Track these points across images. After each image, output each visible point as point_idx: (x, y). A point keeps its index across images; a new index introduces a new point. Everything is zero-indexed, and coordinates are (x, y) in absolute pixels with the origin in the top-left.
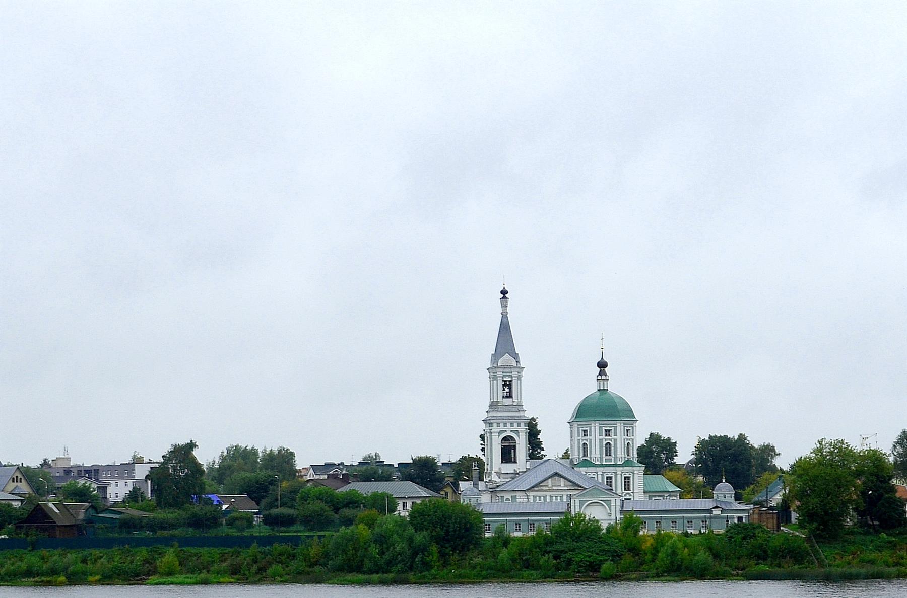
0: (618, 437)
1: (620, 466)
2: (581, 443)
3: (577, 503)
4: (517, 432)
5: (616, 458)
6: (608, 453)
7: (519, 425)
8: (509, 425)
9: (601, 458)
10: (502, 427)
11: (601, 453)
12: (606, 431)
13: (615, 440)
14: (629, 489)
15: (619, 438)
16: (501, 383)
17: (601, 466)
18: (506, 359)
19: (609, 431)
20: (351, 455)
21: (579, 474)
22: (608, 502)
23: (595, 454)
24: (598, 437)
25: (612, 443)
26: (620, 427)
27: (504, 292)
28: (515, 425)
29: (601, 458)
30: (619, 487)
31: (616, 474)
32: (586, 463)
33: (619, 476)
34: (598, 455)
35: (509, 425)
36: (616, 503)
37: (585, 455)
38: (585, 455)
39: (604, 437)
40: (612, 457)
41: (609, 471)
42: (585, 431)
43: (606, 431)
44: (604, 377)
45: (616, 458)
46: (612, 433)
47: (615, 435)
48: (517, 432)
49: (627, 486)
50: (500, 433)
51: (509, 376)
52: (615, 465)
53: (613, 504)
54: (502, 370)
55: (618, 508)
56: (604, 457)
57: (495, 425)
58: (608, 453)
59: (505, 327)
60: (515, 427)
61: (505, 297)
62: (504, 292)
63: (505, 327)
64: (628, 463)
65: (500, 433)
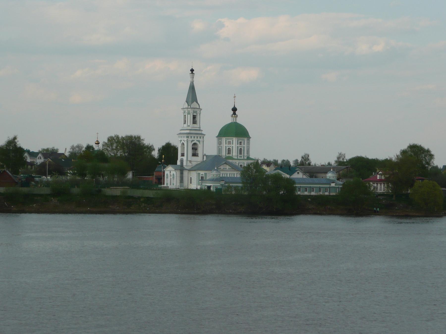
2: (227, 148)
4: (199, 141)
5: (244, 156)
6: (241, 153)
7: (200, 138)
9: (238, 155)
10: (193, 139)
11: (238, 153)
13: (244, 147)
17: (238, 159)
18: (194, 105)
20: (293, 156)
25: (243, 148)
27: (192, 70)
28: (199, 137)
29: (238, 155)
31: (244, 163)
35: (196, 137)
37: (229, 153)
38: (229, 153)
45: (244, 156)
46: (242, 143)
47: (244, 144)
48: (199, 141)
50: (192, 141)
52: (244, 159)
54: (193, 110)
56: (239, 155)
57: (190, 137)
58: (241, 153)
59: (192, 88)
61: (192, 73)
62: (192, 70)
63: (192, 88)
65: (192, 141)
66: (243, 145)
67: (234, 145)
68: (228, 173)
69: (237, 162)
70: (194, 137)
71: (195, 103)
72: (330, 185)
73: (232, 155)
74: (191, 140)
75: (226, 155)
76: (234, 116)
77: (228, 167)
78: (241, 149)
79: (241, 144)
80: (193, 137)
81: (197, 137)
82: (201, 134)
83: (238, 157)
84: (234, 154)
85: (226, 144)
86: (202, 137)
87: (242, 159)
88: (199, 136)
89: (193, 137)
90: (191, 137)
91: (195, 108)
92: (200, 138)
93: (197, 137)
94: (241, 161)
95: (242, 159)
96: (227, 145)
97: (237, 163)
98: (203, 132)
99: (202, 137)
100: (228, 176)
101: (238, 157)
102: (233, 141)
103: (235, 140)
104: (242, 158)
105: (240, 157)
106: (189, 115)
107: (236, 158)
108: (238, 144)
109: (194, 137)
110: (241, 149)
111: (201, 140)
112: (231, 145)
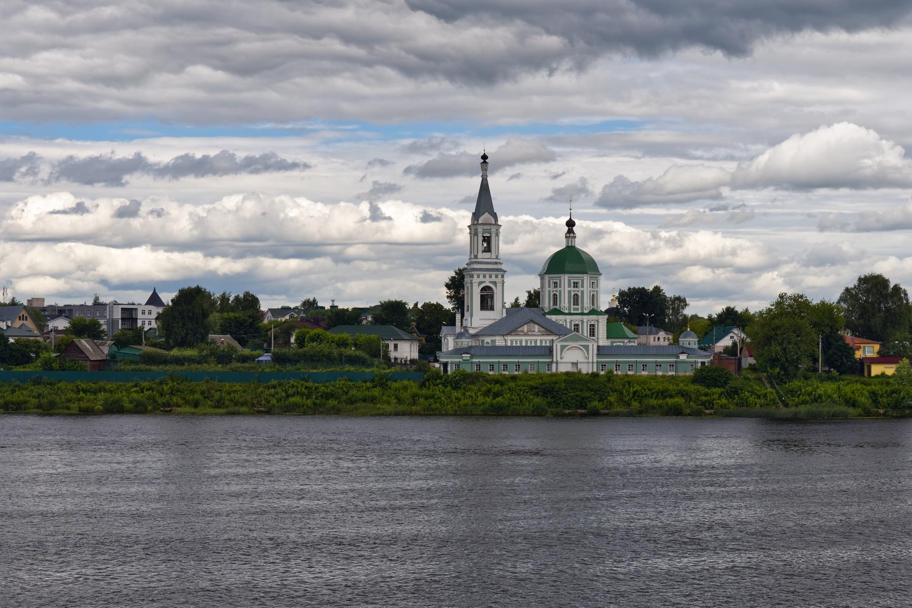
0: (585, 289)
1: (586, 314)
3: (559, 348)
4: (495, 283)
5: (582, 307)
6: (576, 302)
7: (497, 276)
10: (481, 279)
13: (582, 292)
14: (594, 335)
15: (586, 290)
16: (481, 239)
17: (570, 314)
18: (485, 217)
21: (550, 320)
22: (587, 347)
23: (565, 303)
24: (567, 289)
25: (580, 294)
26: (586, 278)
28: (493, 276)
30: (586, 332)
31: (582, 322)
33: (585, 324)
34: (567, 305)
36: (593, 347)
37: (555, 303)
38: (555, 303)
39: (572, 289)
40: (579, 307)
41: (577, 319)
42: (555, 283)
47: (583, 286)
48: (495, 283)
49: (592, 333)
50: (480, 283)
52: (582, 314)
53: (590, 348)
55: (595, 352)
56: (572, 307)
57: (475, 276)
58: (576, 302)
60: (494, 279)
61: (485, 162)
64: (593, 312)
65: (480, 283)
67: (562, 289)
68: (539, 338)
69: (569, 318)
70: (484, 276)
71: (486, 215)
72: (678, 357)
74: (479, 280)
79: (556, 287)
80: (481, 276)
81: (490, 276)
82: (498, 270)
86: (500, 276)
88: (494, 274)
89: (481, 276)
90: (478, 276)
92: (497, 276)
93: (490, 276)
97: (568, 320)
98: (503, 267)
99: (500, 276)
100: (538, 344)
103: (565, 278)
107: (567, 311)
108: (569, 286)
109: (484, 276)
111: (500, 279)
112: (558, 289)
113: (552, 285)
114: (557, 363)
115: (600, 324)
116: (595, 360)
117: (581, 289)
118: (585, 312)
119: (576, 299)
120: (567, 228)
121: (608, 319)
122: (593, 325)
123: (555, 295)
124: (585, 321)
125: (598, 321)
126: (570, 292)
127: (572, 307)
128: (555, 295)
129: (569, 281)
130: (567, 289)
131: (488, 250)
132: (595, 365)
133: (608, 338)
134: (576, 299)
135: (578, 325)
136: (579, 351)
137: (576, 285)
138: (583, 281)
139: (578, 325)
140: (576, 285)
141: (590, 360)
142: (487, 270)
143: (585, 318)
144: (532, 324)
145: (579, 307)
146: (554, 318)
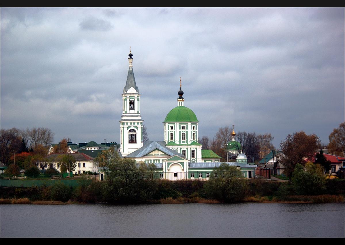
0: (189, 130)
2: (170, 133)
4: (137, 127)
5: (187, 141)
6: (184, 138)
7: (138, 123)
8: (132, 123)
9: (180, 141)
10: (129, 125)
12: (182, 127)
13: (187, 132)
14: (194, 157)
16: (128, 102)
17: (180, 145)
19: (184, 127)
21: (169, 149)
22: (182, 164)
23: (177, 138)
24: (178, 130)
25: (186, 133)
27: (131, 55)
28: (136, 123)
29: (180, 141)
30: (189, 155)
31: (187, 149)
32: (173, 144)
33: (189, 150)
34: (178, 140)
35: (132, 123)
36: (186, 163)
37: (172, 138)
38: (172, 138)
39: (181, 130)
40: (186, 140)
42: (172, 127)
43: (182, 127)
44: (181, 99)
45: (187, 141)
46: (185, 128)
47: (187, 129)
50: (128, 128)
51: (133, 98)
53: (185, 164)
54: (129, 95)
55: (188, 167)
56: (182, 140)
57: (125, 123)
58: (184, 138)
60: (136, 125)
62: (131, 55)
64: (193, 143)
65: (128, 128)
66: (186, 130)
67: (175, 130)
69: (179, 147)
70: (131, 123)
73: (174, 141)
74: (127, 126)
75: (169, 141)
76: (179, 100)
77: (160, 153)
78: (183, 134)
80: (129, 123)
81: (134, 123)
83: (180, 142)
84: (176, 140)
85: (168, 129)
87: (185, 145)
89: (129, 123)
90: (127, 124)
91: (132, 94)
93: (134, 123)
94: (182, 147)
95: (185, 145)
96: (169, 130)
97: (179, 148)
101: (180, 142)
102: (174, 125)
103: (177, 125)
104: (186, 143)
105: (183, 142)
106: (126, 101)
107: (178, 143)
108: (180, 129)
109: (131, 123)
110: (183, 134)
112: (173, 130)
113: (170, 128)
114: (165, 173)
115: (198, 150)
116: (188, 171)
117: (187, 130)
118: (189, 143)
119: (183, 136)
120: (179, 96)
121: (202, 147)
122: (194, 151)
123: (171, 134)
124: (189, 148)
125: (196, 148)
126: (180, 132)
127: (182, 140)
128: (171, 134)
129: (180, 126)
130: (178, 130)
131: (132, 108)
132: (188, 174)
133: (202, 158)
134: (183, 136)
135: (185, 151)
136: (178, 166)
137: (183, 128)
138: (187, 126)
139: (185, 151)
140: (183, 128)
141: (185, 171)
142: (132, 120)
143: (189, 147)
144: (157, 151)
145: (186, 140)
146: (170, 147)
